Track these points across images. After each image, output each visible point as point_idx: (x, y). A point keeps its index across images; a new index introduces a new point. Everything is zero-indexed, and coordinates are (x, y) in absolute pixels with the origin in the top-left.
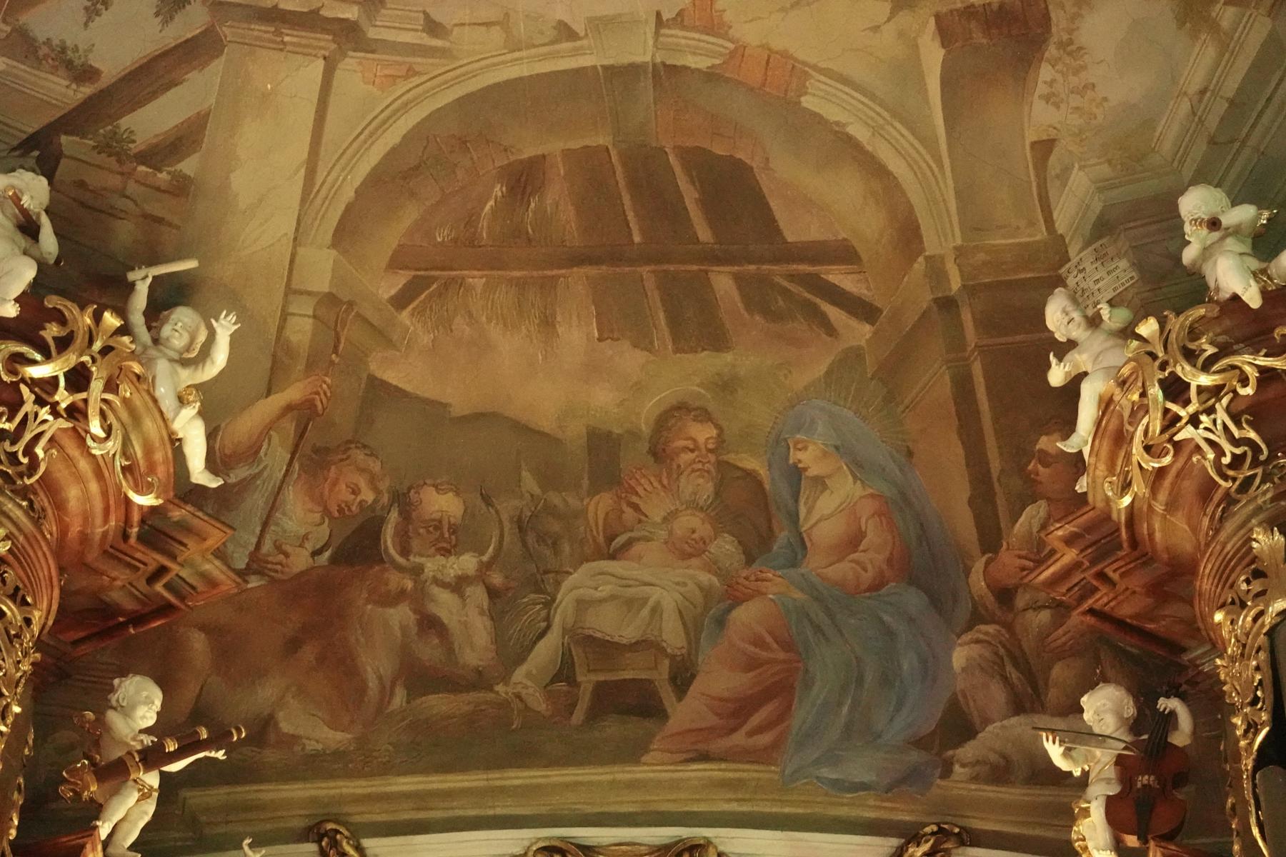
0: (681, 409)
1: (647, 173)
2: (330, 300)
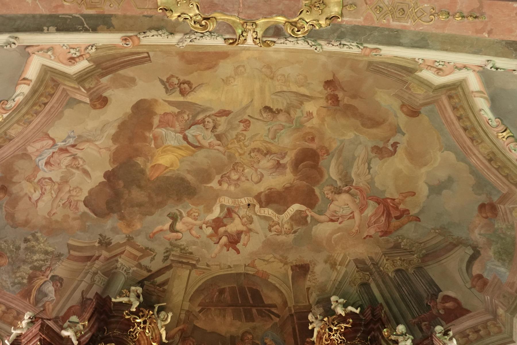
0: (246, 332)
1: (242, 291)
2: (188, 311)
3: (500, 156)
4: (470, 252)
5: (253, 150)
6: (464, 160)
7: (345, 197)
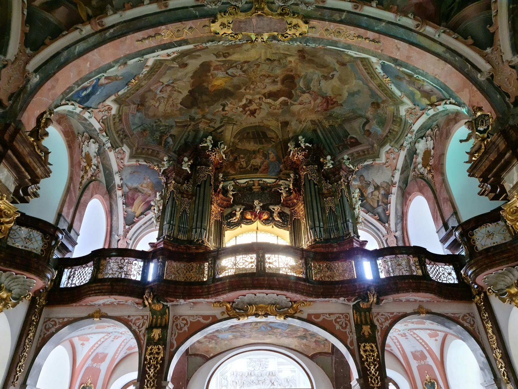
3: (384, 85)
4: (365, 120)
5: (262, 75)
6: (366, 85)
7: (307, 95)
